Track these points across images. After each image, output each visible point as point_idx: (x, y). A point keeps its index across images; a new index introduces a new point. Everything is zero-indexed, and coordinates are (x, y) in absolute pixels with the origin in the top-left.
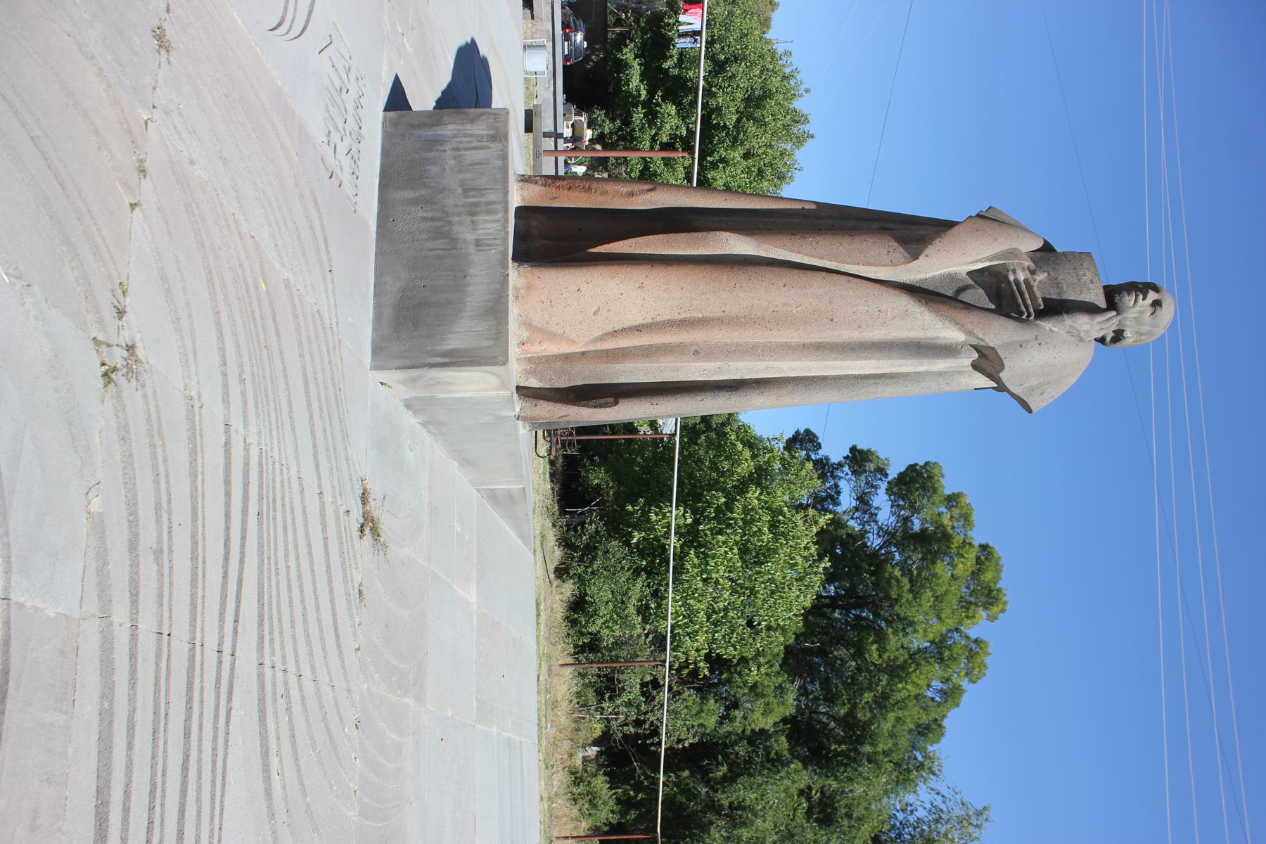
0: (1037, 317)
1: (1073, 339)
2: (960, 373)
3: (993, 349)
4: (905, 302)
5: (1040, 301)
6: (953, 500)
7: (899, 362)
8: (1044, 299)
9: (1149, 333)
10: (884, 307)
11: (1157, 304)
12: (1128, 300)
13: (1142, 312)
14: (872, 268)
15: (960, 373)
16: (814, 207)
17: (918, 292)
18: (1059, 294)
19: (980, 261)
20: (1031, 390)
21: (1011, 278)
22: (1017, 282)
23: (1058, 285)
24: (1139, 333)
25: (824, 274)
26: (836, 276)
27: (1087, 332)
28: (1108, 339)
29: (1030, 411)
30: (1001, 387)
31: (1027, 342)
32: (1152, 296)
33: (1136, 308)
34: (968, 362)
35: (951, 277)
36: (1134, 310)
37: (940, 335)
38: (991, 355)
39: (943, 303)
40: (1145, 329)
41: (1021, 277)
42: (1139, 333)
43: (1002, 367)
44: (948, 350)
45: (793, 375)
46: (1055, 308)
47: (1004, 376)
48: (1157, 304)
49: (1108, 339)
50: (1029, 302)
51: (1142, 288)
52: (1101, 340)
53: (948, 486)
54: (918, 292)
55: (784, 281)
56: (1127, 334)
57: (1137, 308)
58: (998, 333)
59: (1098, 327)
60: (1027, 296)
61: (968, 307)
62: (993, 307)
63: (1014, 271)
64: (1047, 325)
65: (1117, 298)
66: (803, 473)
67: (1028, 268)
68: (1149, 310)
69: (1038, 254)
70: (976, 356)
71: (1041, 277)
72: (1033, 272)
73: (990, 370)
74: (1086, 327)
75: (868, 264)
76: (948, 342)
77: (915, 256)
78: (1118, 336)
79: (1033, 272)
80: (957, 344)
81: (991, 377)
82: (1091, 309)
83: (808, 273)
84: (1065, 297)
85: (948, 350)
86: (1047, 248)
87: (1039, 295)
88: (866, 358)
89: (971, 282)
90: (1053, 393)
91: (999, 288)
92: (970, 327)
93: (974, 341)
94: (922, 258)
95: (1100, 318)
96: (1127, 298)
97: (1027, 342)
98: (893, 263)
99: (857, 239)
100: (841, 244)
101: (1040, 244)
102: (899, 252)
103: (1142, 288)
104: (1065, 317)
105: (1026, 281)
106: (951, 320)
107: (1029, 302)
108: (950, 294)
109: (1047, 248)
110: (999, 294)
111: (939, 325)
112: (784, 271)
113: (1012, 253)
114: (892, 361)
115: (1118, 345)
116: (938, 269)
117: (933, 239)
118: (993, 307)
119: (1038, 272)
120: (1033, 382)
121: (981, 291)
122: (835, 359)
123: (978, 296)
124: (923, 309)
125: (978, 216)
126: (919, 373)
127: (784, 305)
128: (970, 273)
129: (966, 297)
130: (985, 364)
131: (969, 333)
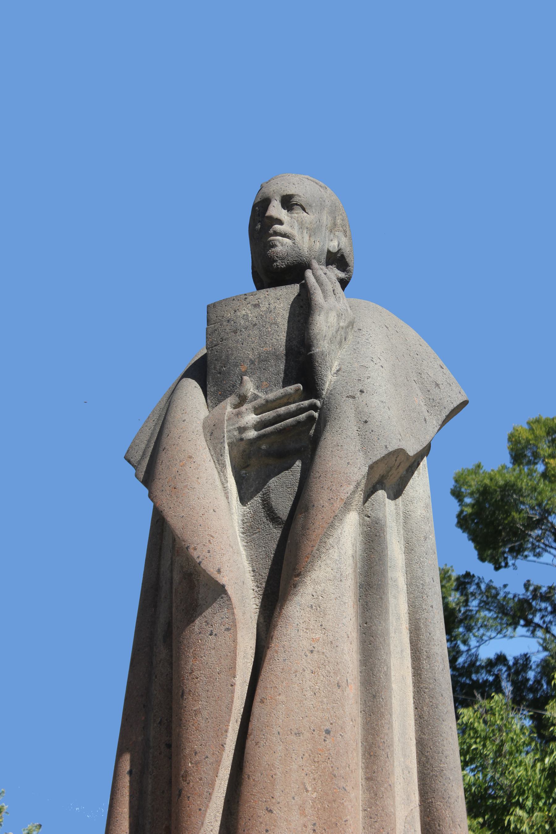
0: (317, 396)
1: (350, 337)
2: (407, 517)
3: (371, 467)
4: (298, 609)
5: (291, 389)
6: (520, 453)
7: (392, 619)
8: (286, 382)
9: (333, 212)
10: (306, 644)
11: (288, 202)
12: (282, 247)
13: (302, 225)
14: (240, 662)
15: (407, 517)
16: (127, 759)
17: (278, 586)
18: (277, 358)
19: (224, 483)
20: (432, 403)
21: (252, 434)
22: (259, 426)
23: (263, 359)
24: (333, 228)
25: (250, 743)
26: (254, 723)
27: (339, 316)
28: (342, 275)
29: (464, 404)
30: (426, 451)
31: (359, 412)
32: (276, 210)
33: (295, 235)
34: (390, 505)
35: (250, 530)
36: (298, 238)
37: (350, 552)
38: (381, 470)
39: (297, 547)
40: (326, 219)
41: (251, 418)
42: (333, 228)
43: (400, 452)
44: (373, 539)
45: (416, 798)
46: (301, 364)
47: (412, 450)
48: (288, 202)
49: (342, 275)
50: (293, 407)
51: (261, 226)
52: (344, 283)
53: (495, 460)
54: (278, 586)
55: (262, 812)
56: (333, 246)
57: (295, 232)
58: (345, 459)
59: (332, 299)
60: (282, 410)
61: (301, 501)
62: (298, 463)
63: (242, 430)
64: (329, 380)
65: (279, 264)
66: (480, 726)
67: (236, 406)
68: (298, 214)
69: (211, 389)
70: (381, 494)
71: (250, 386)
72: (243, 400)
73: (402, 471)
74: (332, 318)
75: (232, 669)
76: (360, 538)
77: (220, 591)
78: (337, 260)
79: (243, 400)
80: (362, 524)
81: (413, 465)
82: (303, 311)
83: (249, 769)
84: (282, 349)
85: (373, 539)
86: (200, 371)
87: (278, 392)
88: (387, 675)
89: (257, 499)
90: (435, 368)
91: (268, 454)
92: (338, 504)
93: (359, 497)
94: (223, 579)
95: (318, 297)
96: (279, 248)
97: (359, 412)
98: (232, 628)
99: (189, 685)
100: (197, 712)
101: (192, 388)
102: (211, 618)
103: (261, 226)
104: (316, 350)
105: (258, 411)
106: (327, 535)
107: (293, 407)
108: (277, 533)
109: (200, 371)
110: (283, 453)
111: (334, 554)
112: (245, 812)
113: (212, 431)
114: (392, 629)
115: (350, 260)
116: (239, 553)
117: (189, 559)
118: (298, 463)
119: (243, 391)
120: (419, 400)
121: (273, 482)
122: (391, 728)
123: (282, 488)
124: (308, 580)
125: (148, 479)
126: (409, 585)
127: (303, 813)
128: (243, 499)
129: (283, 506)
130: (392, 480)
131: (347, 506)
